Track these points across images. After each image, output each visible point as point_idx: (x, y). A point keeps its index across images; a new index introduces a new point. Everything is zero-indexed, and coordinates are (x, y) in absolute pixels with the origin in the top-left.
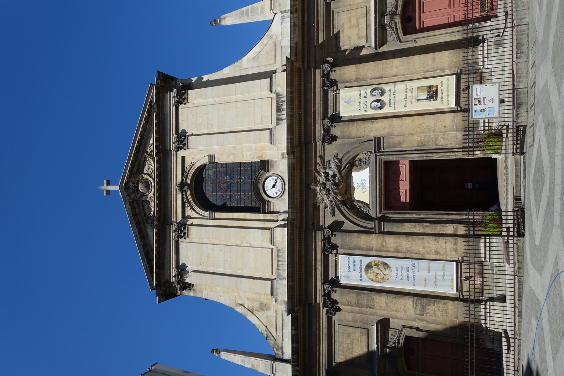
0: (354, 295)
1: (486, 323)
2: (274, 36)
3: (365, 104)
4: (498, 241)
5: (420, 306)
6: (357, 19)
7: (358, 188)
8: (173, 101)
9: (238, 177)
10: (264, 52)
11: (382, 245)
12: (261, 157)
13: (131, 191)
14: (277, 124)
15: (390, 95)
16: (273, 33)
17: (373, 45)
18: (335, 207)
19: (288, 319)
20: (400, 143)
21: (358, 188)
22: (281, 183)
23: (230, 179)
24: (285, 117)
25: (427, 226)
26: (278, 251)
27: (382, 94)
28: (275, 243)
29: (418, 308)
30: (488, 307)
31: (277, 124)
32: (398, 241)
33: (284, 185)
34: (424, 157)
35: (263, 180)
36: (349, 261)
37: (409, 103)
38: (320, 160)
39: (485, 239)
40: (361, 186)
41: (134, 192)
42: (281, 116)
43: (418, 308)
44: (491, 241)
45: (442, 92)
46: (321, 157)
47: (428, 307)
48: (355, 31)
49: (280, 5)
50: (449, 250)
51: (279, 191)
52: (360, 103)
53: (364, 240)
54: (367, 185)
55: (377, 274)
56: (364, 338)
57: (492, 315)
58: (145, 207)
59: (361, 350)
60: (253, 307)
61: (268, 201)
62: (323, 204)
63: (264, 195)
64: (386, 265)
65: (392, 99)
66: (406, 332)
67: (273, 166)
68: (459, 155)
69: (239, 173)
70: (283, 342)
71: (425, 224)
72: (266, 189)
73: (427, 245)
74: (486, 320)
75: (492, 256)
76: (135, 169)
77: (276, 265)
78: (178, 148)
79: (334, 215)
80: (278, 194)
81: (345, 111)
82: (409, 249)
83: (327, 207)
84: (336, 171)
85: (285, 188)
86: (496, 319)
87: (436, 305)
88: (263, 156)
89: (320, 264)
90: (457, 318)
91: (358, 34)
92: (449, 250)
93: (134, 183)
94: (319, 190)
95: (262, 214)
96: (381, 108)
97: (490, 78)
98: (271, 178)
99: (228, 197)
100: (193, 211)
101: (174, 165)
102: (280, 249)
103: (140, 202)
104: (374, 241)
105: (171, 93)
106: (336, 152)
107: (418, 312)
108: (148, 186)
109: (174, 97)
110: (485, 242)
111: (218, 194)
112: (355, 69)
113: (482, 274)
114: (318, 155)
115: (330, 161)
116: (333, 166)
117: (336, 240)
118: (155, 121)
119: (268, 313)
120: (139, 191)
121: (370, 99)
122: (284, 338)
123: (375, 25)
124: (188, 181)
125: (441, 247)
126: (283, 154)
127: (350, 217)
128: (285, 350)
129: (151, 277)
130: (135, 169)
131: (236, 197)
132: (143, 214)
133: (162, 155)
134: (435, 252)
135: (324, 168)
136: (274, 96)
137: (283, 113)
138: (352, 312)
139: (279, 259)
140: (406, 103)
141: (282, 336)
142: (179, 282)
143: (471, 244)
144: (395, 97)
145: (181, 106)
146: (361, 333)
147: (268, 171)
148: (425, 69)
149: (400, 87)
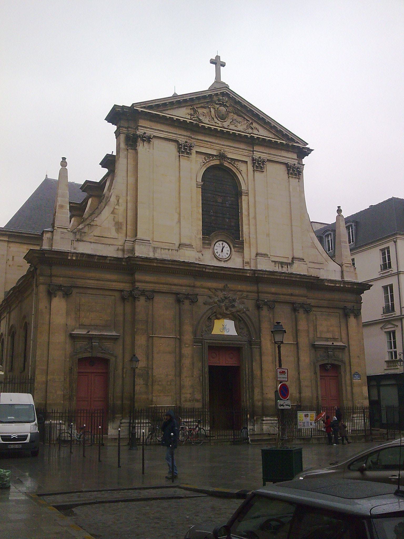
5: (141, 373)
7: (223, 325)
9: (228, 216)
13: (221, 98)
21: (223, 325)
25: (200, 379)
28: (182, 249)
29: (140, 371)
31: (272, 261)
33: (224, 260)
38: (245, 296)
41: (219, 100)
43: (140, 371)
46: (247, 296)
53: (188, 329)
54: (226, 333)
59: (92, 320)
61: (210, 244)
63: (216, 241)
66: (112, 359)
67: (238, 252)
71: (201, 378)
80: (216, 254)
83: (211, 299)
85: (222, 261)
87: (144, 385)
95: (202, 237)
114: (250, 294)
116: (242, 306)
117: (186, 305)
118: (279, 141)
119: (113, 229)
122: (92, 244)
124: (226, 164)
126: (248, 263)
128: (81, 243)
131: (211, 211)
132: (199, 106)
133: (250, 140)
135: (239, 299)
136: (290, 261)
139: (170, 250)
145: (283, 168)
147: (234, 247)
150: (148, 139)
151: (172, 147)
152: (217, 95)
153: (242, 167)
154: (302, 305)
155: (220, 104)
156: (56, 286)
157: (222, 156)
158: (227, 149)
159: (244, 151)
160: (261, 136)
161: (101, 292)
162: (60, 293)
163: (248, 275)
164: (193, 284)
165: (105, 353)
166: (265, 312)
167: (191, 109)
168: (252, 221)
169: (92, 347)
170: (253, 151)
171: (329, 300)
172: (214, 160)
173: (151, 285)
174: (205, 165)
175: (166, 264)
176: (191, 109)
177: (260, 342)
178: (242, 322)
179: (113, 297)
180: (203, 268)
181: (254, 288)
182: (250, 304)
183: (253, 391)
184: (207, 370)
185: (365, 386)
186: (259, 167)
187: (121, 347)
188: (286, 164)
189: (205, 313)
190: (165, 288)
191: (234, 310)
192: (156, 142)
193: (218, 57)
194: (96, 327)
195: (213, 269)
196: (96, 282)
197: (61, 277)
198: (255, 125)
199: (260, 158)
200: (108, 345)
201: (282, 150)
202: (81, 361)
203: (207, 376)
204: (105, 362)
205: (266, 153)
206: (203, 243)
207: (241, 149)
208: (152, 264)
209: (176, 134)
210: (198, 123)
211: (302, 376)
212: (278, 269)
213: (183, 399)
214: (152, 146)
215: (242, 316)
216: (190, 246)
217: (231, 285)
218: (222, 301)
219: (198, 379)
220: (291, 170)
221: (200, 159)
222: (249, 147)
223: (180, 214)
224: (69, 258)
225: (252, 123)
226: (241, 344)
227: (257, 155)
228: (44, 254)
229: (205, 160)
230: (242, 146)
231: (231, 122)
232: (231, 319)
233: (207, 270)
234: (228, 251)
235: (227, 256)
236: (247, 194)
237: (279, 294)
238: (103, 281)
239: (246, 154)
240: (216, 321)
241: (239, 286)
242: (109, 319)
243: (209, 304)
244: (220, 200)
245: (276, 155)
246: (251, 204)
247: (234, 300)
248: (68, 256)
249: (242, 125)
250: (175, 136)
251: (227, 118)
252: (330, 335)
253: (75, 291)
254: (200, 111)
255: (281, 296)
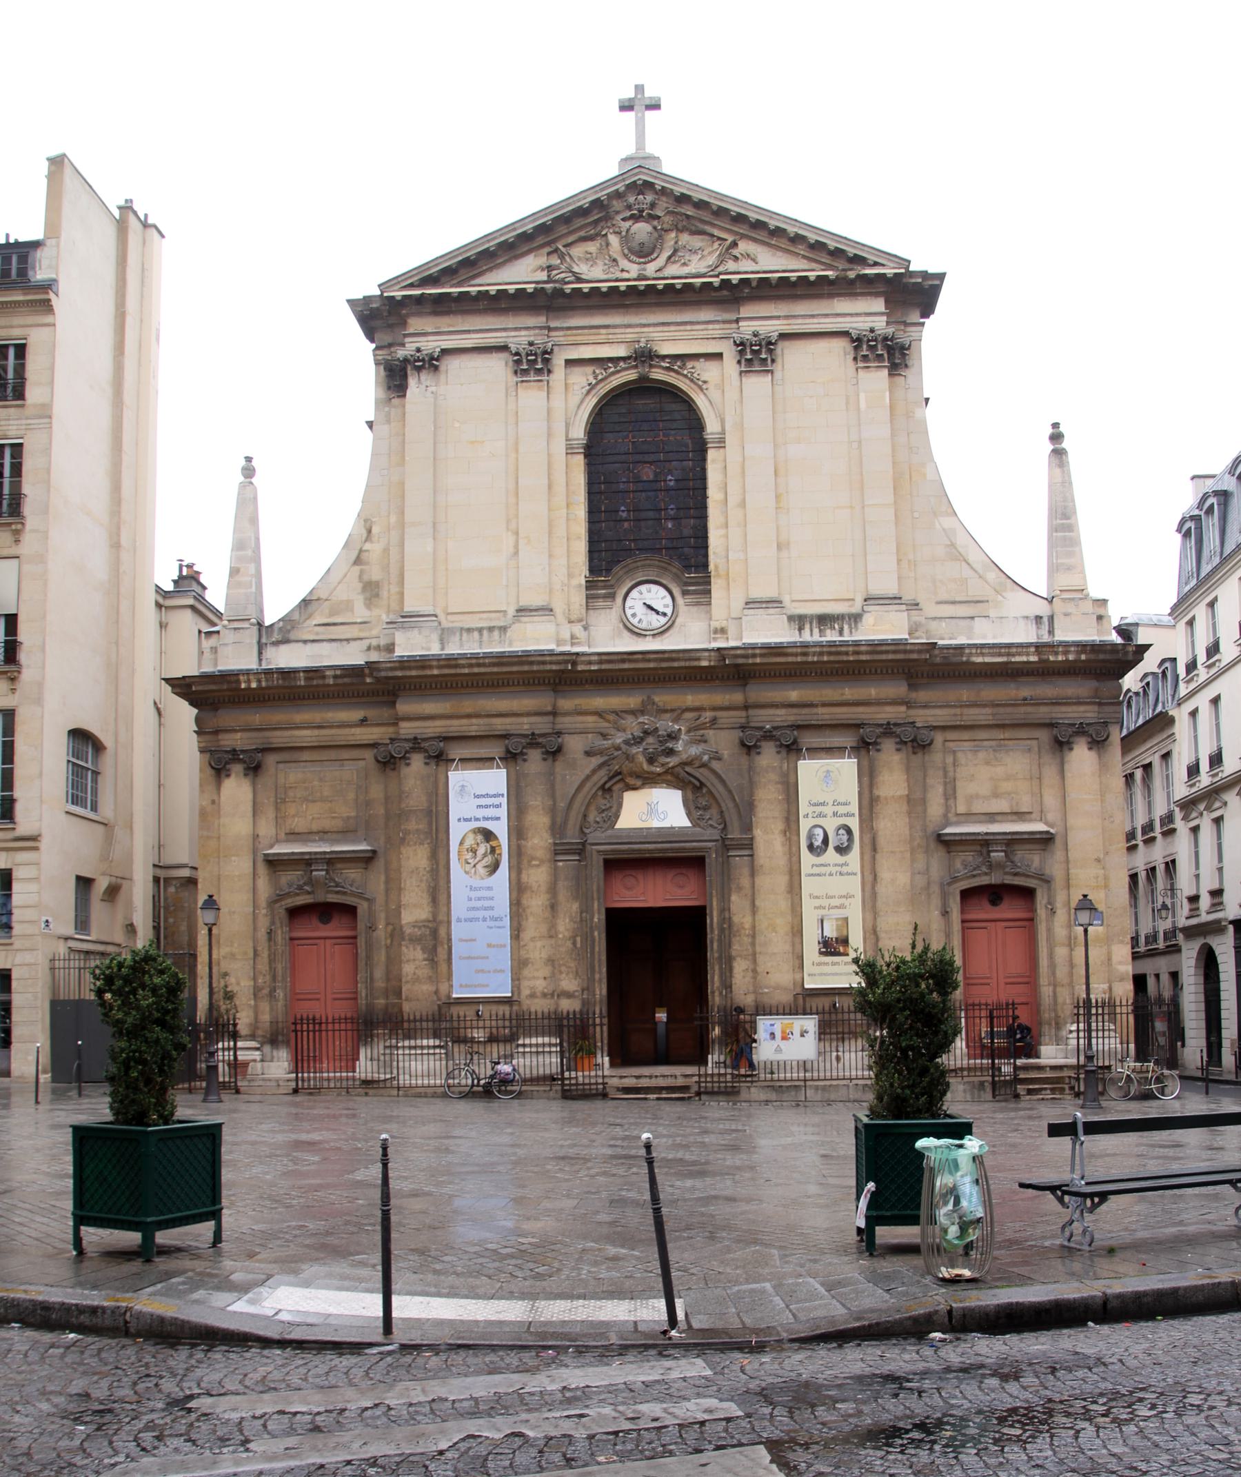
0: (426, 805)
1: (404, 1047)
2: (1000, 598)
3: (820, 815)
4: (554, 1066)
6: (1009, 794)
8: (859, 325)
9: (672, 513)
10: (967, 572)
11: (533, 858)
12: (718, 576)
13: (631, 199)
14: (791, 618)
15: (836, 865)
16: (1009, 595)
17: (948, 830)
18: (606, 758)
19: (353, 656)
20: (740, 889)
22: (659, 625)
23: (668, 490)
24: (807, 637)
25: (574, 943)
26: (503, 629)
27: (841, 850)
28: (519, 621)
30: (437, 1051)
31: (791, 618)
32: (543, 888)
34: (713, 935)
35: (664, 582)
36: (495, 796)
37: (818, 902)
39: (555, 1045)
40: (652, 809)
41: (629, 207)
42: (807, 626)
44: (554, 1055)
45: (834, 964)
46: (714, 720)
47: (419, 948)
48: (985, 789)
49: (1066, 615)
50: (531, 983)
51: (640, 621)
52: (823, 804)
53: (538, 820)
54: (656, 824)
55: (474, 852)
56: (338, 824)
57: (419, 1057)
58: (590, 243)
60: (367, 563)
61: (612, 596)
62: (612, 731)
64: (494, 867)
65: (827, 870)
66: (363, 908)
67: (698, 604)
68: (716, 999)
69: (682, 513)
70: (300, 644)
71: (578, 939)
72: (643, 588)
73: (539, 944)
74: (410, 1048)
75: (528, 1056)
76: (690, 211)
77: (473, 626)
78: (741, 345)
79: (588, 754)
80: (631, 619)
81: (809, 770)
82: (528, 911)
84: (684, 757)
86: (413, 1063)
88: (719, 581)
89: (483, 728)
90: (407, 999)
91: (977, 796)
92: (531, 983)
93: (653, 205)
94: (641, 720)
95: (583, 582)
96: (811, 847)
97: (853, 1049)
98: (668, 600)
99: (622, 486)
100: (584, 391)
101: (699, 330)
102: (508, 634)
103: (603, 228)
104: (539, 841)
105: (885, 318)
106: (726, 756)
107: (408, 931)
108: (644, 253)
109: (872, 330)
110: (550, 1045)
111: (631, 458)
112: (898, 793)
113: (492, 1039)
114: (719, 714)
115: (705, 742)
116: (694, 750)
118: (812, 275)
120: (630, 223)
121: (831, 825)
122: (309, 645)
123: (987, 834)
124: (658, 375)
125: (537, 970)
126: (723, 631)
127: (586, 789)
128: (284, 648)
129: (409, 282)
130: (690, 211)
132: (570, 239)
133: (725, 293)
134: (527, 959)
135: (689, 731)
136: (856, 609)
137: (816, 631)
138: (387, 798)
139: (485, 633)
140: (817, 897)
141: (313, 641)
142: (406, 360)
143: (546, 1022)
144: (831, 875)
146: (348, 818)
147: (685, 593)
148: (882, 935)
149: (854, 885)
150: (430, 363)
151: (498, 366)
152: (618, 195)
153: (709, 371)
154: (888, 730)
155: (632, 217)
156: (227, 752)
157: (645, 356)
158: (655, 333)
159: (711, 326)
160: (753, 273)
161: (333, 754)
162: (237, 768)
163: (705, 663)
164: (549, 708)
165: (345, 893)
166: (768, 757)
167: (549, 254)
168: (734, 514)
169: (310, 882)
170: (737, 321)
171: (998, 705)
172: (619, 372)
173: (438, 723)
174: (594, 392)
175: (463, 666)
176: (549, 254)
177: (752, 839)
178: (704, 790)
179: (362, 763)
180: (566, 662)
181: (737, 697)
182: (724, 742)
183: (731, 969)
184: (599, 918)
185: (1122, 942)
186: (756, 362)
187: (383, 878)
188: (845, 334)
189: (588, 778)
190: (474, 726)
191: (672, 761)
192: (452, 365)
193: (639, 89)
194: (323, 834)
195: (600, 662)
196: (316, 732)
197: (236, 731)
198: (744, 246)
199: (755, 335)
200: (352, 874)
201: (831, 296)
202: (295, 913)
203: (600, 937)
204: (351, 911)
205: (778, 318)
206: (588, 597)
207: (698, 323)
208: (429, 672)
209: (505, 330)
210: (557, 285)
211: (882, 924)
212: (811, 636)
213: (526, 992)
214: (443, 377)
215: (697, 775)
216: (547, 610)
217: (664, 698)
218: (638, 741)
219: (569, 944)
220: (865, 347)
221: (581, 377)
222: (726, 311)
223: (517, 533)
224: (243, 686)
225: (734, 244)
226: (701, 849)
227: (747, 329)
228: (189, 686)
229: (595, 378)
230: (705, 314)
231: (670, 258)
232: (671, 785)
233: (580, 668)
234: (666, 606)
235: (663, 620)
236: (721, 443)
237: (815, 706)
238: (331, 727)
239: (717, 333)
240: (630, 798)
241: (689, 698)
242: (353, 814)
243: (601, 753)
244: (648, 473)
245: (813, 316)
246: (733, 469)
247: (673, 736)
248: (238, 682)
249: (703, 256)
250: (504, 334)
251: (657, 251)
252: (1002, 805)
253: (270, 760)
254: (577, 251)
255: (820, 710)
